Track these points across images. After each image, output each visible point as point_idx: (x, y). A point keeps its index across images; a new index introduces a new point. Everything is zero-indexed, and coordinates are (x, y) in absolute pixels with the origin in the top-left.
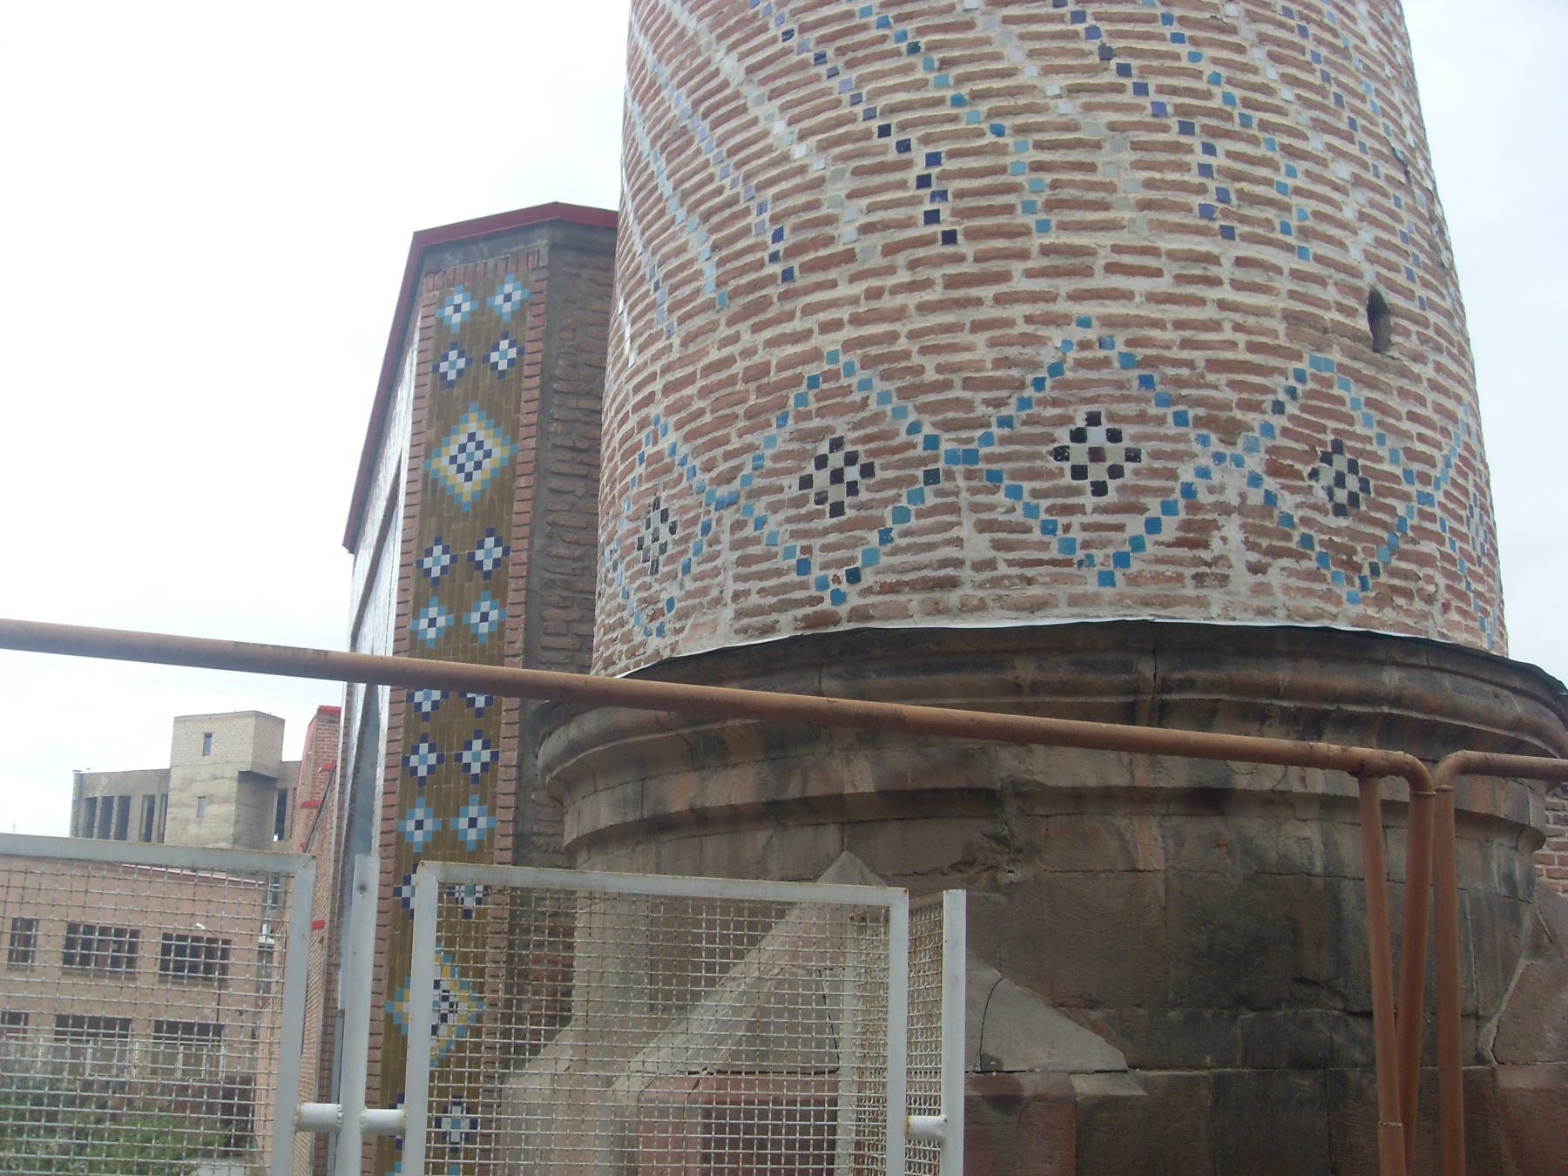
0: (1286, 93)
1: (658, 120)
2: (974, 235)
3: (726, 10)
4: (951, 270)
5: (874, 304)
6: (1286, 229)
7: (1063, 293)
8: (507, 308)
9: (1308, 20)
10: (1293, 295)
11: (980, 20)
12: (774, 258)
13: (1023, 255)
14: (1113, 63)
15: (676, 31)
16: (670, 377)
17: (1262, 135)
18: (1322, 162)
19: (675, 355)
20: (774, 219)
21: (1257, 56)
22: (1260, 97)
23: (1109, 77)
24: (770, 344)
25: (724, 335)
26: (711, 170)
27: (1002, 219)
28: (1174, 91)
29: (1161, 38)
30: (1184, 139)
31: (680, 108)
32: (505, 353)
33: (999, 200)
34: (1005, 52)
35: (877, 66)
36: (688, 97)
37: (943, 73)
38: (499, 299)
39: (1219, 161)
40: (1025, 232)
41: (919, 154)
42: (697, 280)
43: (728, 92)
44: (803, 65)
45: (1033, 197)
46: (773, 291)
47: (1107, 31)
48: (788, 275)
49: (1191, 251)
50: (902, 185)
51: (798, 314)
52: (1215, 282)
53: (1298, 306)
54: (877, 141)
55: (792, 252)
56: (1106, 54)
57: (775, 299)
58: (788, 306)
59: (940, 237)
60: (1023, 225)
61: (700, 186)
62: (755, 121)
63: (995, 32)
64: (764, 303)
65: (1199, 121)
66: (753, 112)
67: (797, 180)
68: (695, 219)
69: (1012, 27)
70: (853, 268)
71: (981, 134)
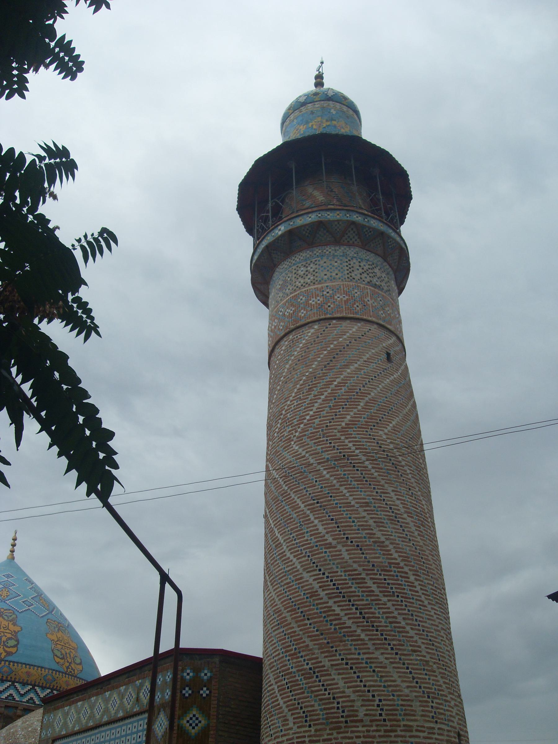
0: (444, 686)
2: (390, 720)
4: (385, 728)
5: (369, 734)
8: (205, 678)
10: (447, 736)
11: (388, 666)
12: (342, 717)
13: (399, 726)
14: (415, 680)
16: (311, 738)
17: (441, 697)
19: (313, 733)
21: (439, 678)
22: (440, 688)
23: (414, 684)
24: (342, 738)
27: (395, 717)
30: (428, 700)
32: (204, 692)
35: (365, 674)
38: (203, 674)
39: (434, 705)
41: (377, 698)
45: (401, 712)
46: (343, 725)
48: (346, 722)
49: (430, 727)
50: (373, 705)
52: (434, 733)
53: (448, 738)
55: (347, 716)
58: (347, 730)
60: (399, 719)
63: (391, 670)
64: (340, 728)
65: (431, 695)
69: (395, 669)
70: (362, 724)
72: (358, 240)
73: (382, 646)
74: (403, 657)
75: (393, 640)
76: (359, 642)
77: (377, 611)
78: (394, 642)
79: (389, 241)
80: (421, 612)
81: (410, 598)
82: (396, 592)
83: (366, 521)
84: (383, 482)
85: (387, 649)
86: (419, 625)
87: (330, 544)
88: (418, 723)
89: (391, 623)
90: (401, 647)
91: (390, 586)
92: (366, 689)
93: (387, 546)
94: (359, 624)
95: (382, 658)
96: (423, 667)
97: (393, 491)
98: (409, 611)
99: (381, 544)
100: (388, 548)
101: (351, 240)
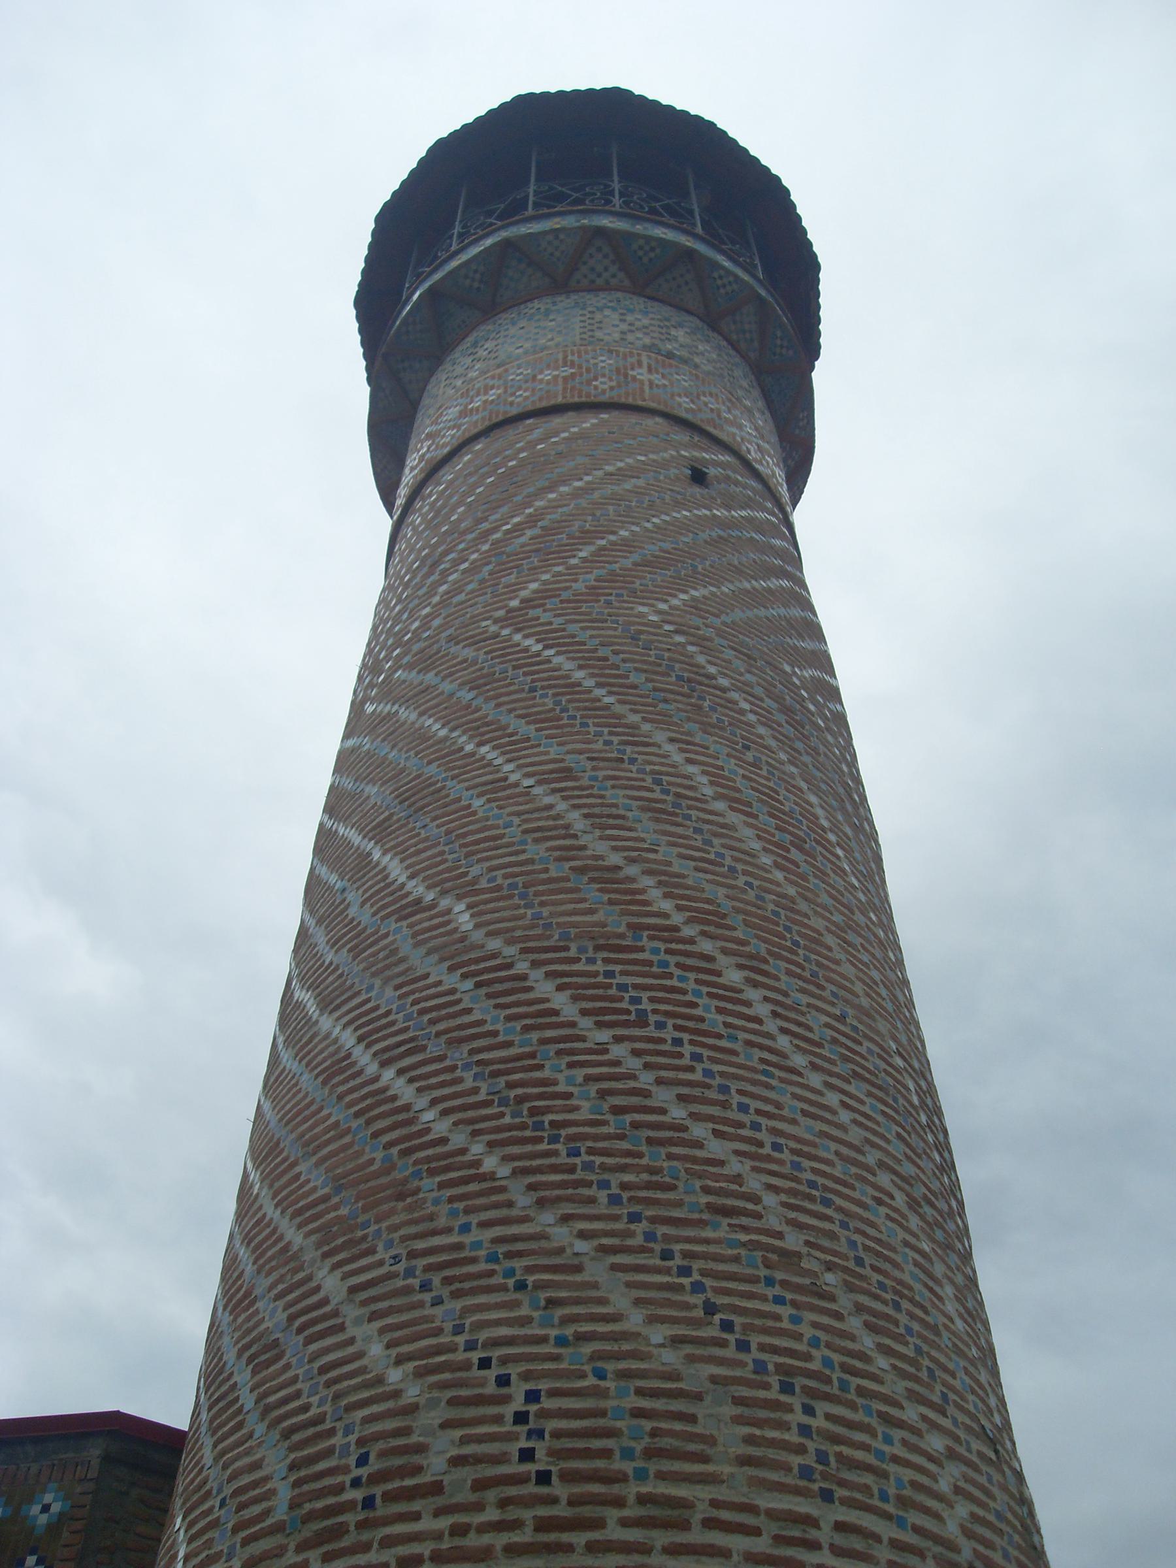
0: (883, 1362)
1: (249, 1331)
2: (568, 1477)
3: (335, 1229)
4: (543, 1511)
5: (458, 1542)
6: (884, 1497)
7: (658, 1545)
9: (902, 1296)
12: (356, 1483)
13: (619, 1502)
14: (717, 1318)
15: (280, 1245)
17: (860, 1401)
18: (917, 1432)
20: (360, 1442)
21: (854, 1324)
22: (858, 1364)
23: (713, 1332)
25: (291, 1561)
26: (299, 1386)
27: (600, 1464)
28: (775, 1350)
29: (764, 1299)
30: (784, 1398)
31: (275, 1320)
33: (597, 1444)
34: (613, 1297)
35: (482, 1299)
36: (285, 1310)
37: (548, 1312)
39: (818, 1422)
40: (622, 1478)
41: (518, 1390)
42: (269, 1499)
43: (327, 1309)
44: (407, 1291)
45: (633, 1444)
46: (350, 1518)
47: (712, 1287)
48: (369, 1503)
49: (790, 1512)
50: (498, 1419)
51: (375, 1545)
54: (476, 1373)
55: (375, 1479)
56: (710, 1309)
57: (352, 1528)
58: (365, 1536)
59: (533, 1476)
60: (620, 1471)
61: (285, 1401)
62: (351, 1341)
64: (339, 1531)
65: (799, 1382)
66: (351, 1331)
67: (390, 1404)
68: (276, 1435)
70: (440, 1501)
71: (583, 1376)
72: (621, 275)
73: (570, 1191)
74: (662, 1230)
75: (623, 1169)
76: (473, 1187)
77: (561, 1077)
78: (628, 1178)
79: (716, 275)
80: (768, 1086)
81: (719, 1036)
82: (655, 1011)
83: (558, 817)
84: (634, 718)
85: (592, 1201)
86: (756, 1127)
87: (418, 901)
88: (722, 1493)
89: (617, 1110)
90: (659, 1195)
91: (627, 996)
92: (475, 1356)
93: (632, 880)
94: (477, 1127)
95: (561, 1235)
96: (763, 1272)
97: (672, 740)
98: (708, 1073)
99: (606, 877)
100: (634, 886)
101: (599, 275)
